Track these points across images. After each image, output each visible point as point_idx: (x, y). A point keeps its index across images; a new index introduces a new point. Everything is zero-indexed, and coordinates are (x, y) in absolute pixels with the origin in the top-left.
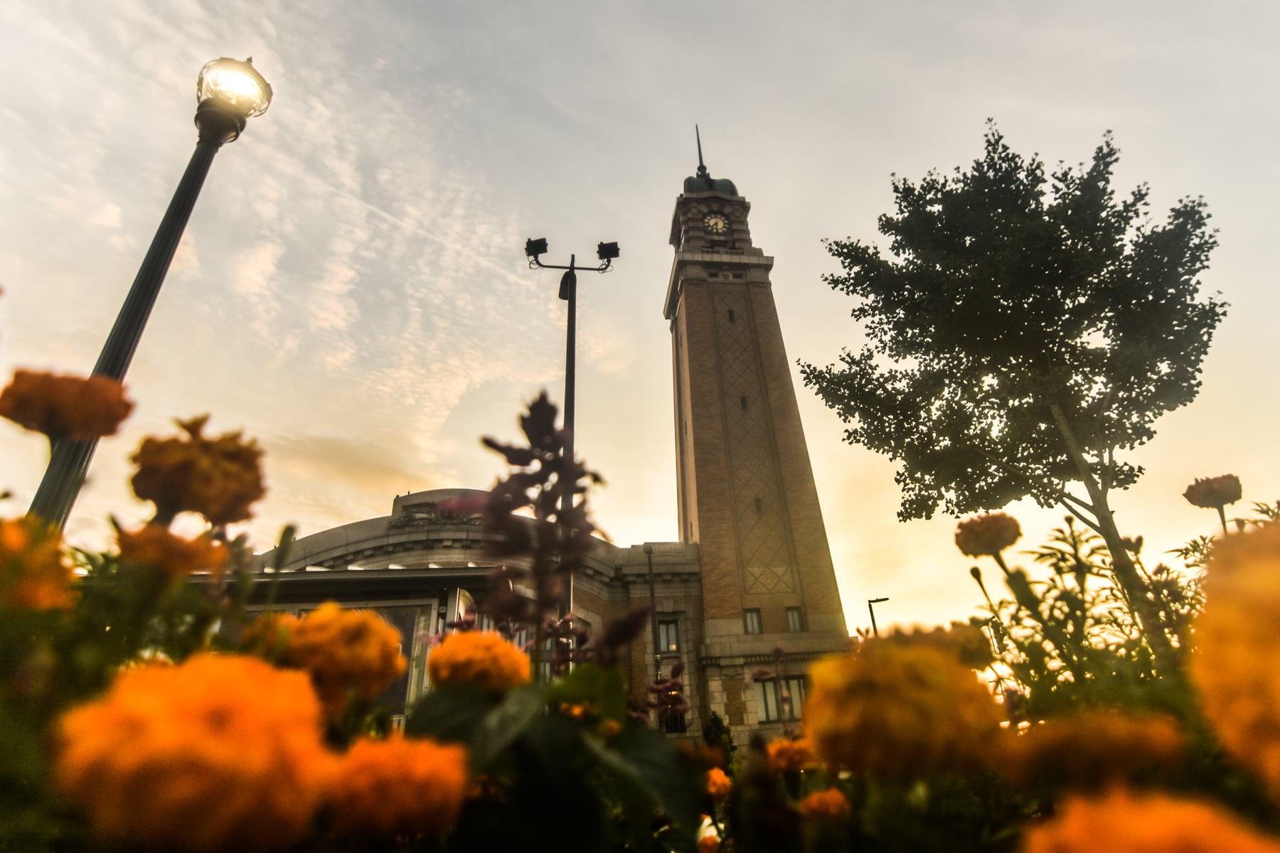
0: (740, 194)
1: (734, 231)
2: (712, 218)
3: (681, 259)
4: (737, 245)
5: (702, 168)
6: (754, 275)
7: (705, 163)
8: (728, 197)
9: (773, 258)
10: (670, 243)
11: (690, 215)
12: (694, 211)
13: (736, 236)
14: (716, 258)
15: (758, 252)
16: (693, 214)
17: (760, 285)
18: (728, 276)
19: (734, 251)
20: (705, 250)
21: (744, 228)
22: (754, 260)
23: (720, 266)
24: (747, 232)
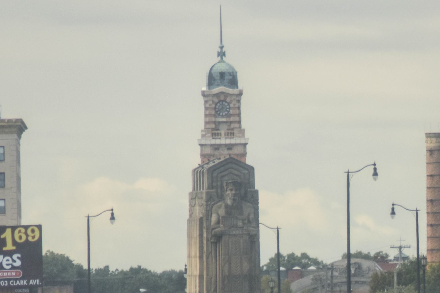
5: (222, 47)
8: (230, 91)
13: (232, 119)
14: (218, 142)
15: (242, 132)
19: (230, 131)
23: (220, 145)
24: (239, 115)
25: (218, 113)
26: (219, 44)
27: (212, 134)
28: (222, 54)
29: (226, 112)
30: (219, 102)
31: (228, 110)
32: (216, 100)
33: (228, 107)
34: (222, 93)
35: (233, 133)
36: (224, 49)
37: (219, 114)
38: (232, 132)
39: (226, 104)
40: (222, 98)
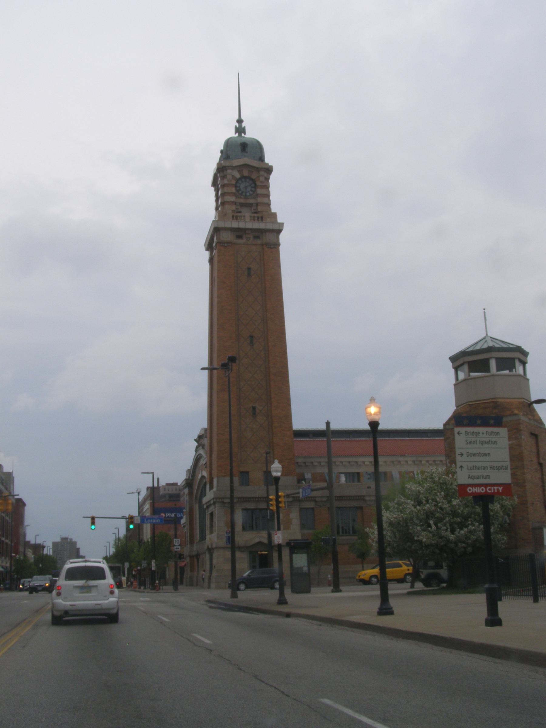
0: (267, 161)
1: (258, 195)
2: (242, 182)
3: (216, 226)
4: (260, 208)
5: (240, 121)
6: (269, 237)
7: (242, 118)
8: (255, 164)
9: (283, 224)
10: (212, 186)
11: (226, 181)
12: (229, 177)
16: (228, 181)
17: (272, 247)
18: (249, 238)
19: (256, 215)
20: (235, 214)
21: (265, 200)
22: (269, 226)
23: (244, 230)
24: (268, 195)
25: (240, 192)
26: (237, 118)
27: (233, 216)
28: (240, 130)
29: (251, 193)
30: (240, 179)
31: (253, 189)
32: (238, 176)
33: (253, 185)
34: (246, 166)
35: (262, 218)
36: (243, 125)
37: (241, 194)
38: (260, 215)
39: (251, 182)
40: (246, 173)
